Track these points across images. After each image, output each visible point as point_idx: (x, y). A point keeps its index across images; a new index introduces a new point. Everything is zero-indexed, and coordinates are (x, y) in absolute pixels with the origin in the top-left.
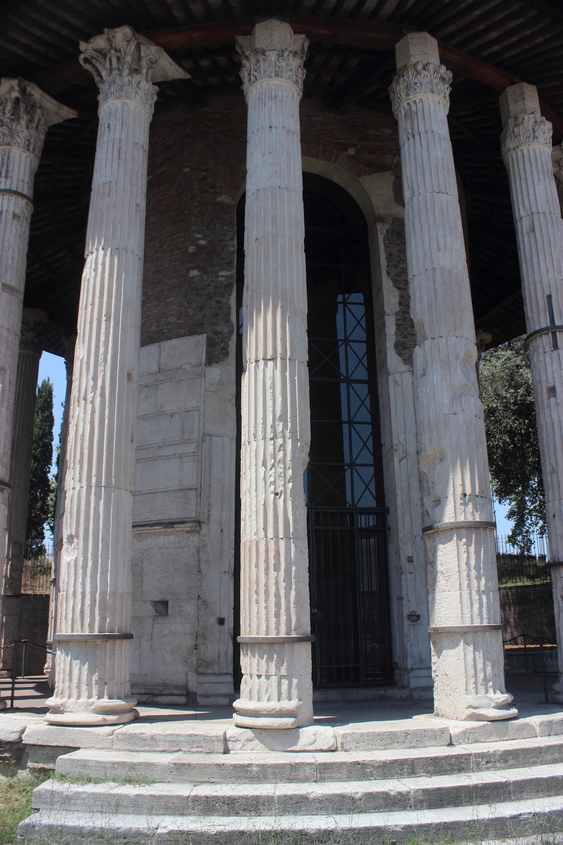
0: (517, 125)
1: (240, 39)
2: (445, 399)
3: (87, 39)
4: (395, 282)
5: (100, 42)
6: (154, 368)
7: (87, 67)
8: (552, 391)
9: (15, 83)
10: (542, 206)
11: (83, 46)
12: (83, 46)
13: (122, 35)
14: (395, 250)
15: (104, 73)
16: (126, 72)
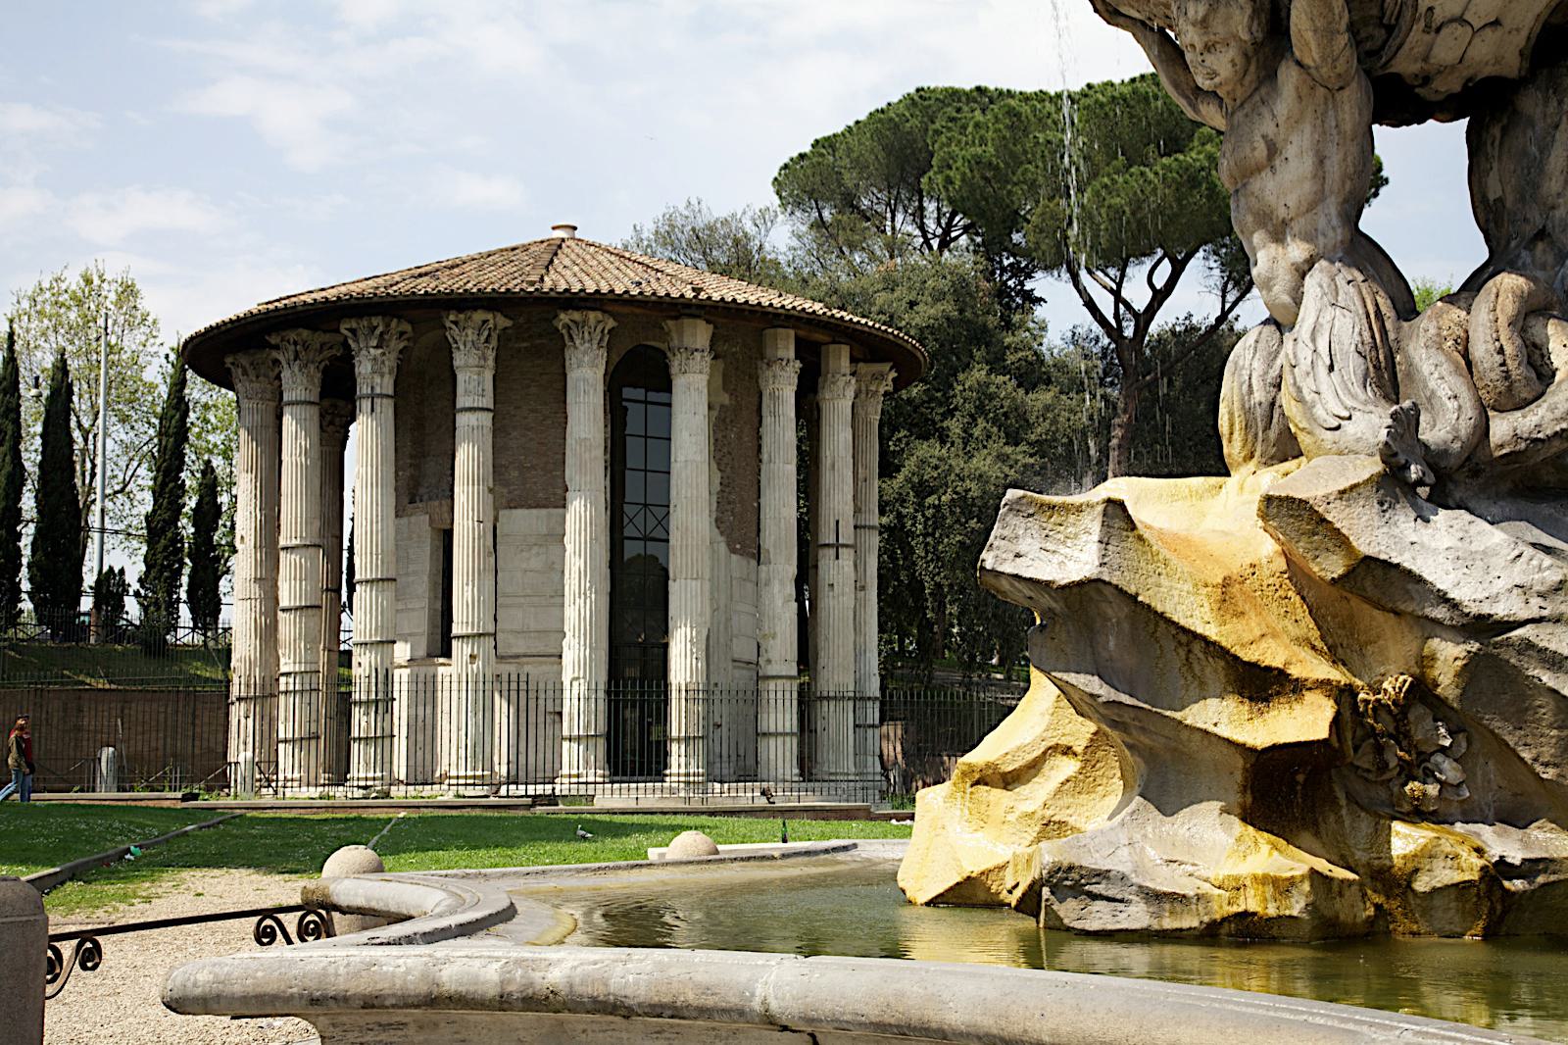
0: (833, 383)
1: (670, 323)
2: (779, 603)
3: (565, 309)
4: (718, 464)
5: (577, 316)
6: (544, 531)
7: (564, 331)
8: (832, 585)
9: (490, 316)
10: (842, 453)
11: (562, 316)
12: (562, 316)
13: (593, 316)
14: (720, 436)
15: (578, 342)
16: (595, 346)
